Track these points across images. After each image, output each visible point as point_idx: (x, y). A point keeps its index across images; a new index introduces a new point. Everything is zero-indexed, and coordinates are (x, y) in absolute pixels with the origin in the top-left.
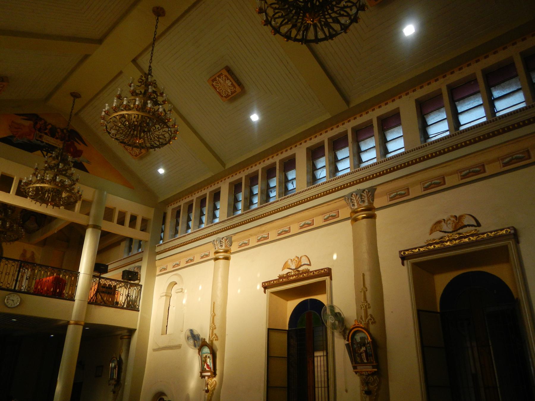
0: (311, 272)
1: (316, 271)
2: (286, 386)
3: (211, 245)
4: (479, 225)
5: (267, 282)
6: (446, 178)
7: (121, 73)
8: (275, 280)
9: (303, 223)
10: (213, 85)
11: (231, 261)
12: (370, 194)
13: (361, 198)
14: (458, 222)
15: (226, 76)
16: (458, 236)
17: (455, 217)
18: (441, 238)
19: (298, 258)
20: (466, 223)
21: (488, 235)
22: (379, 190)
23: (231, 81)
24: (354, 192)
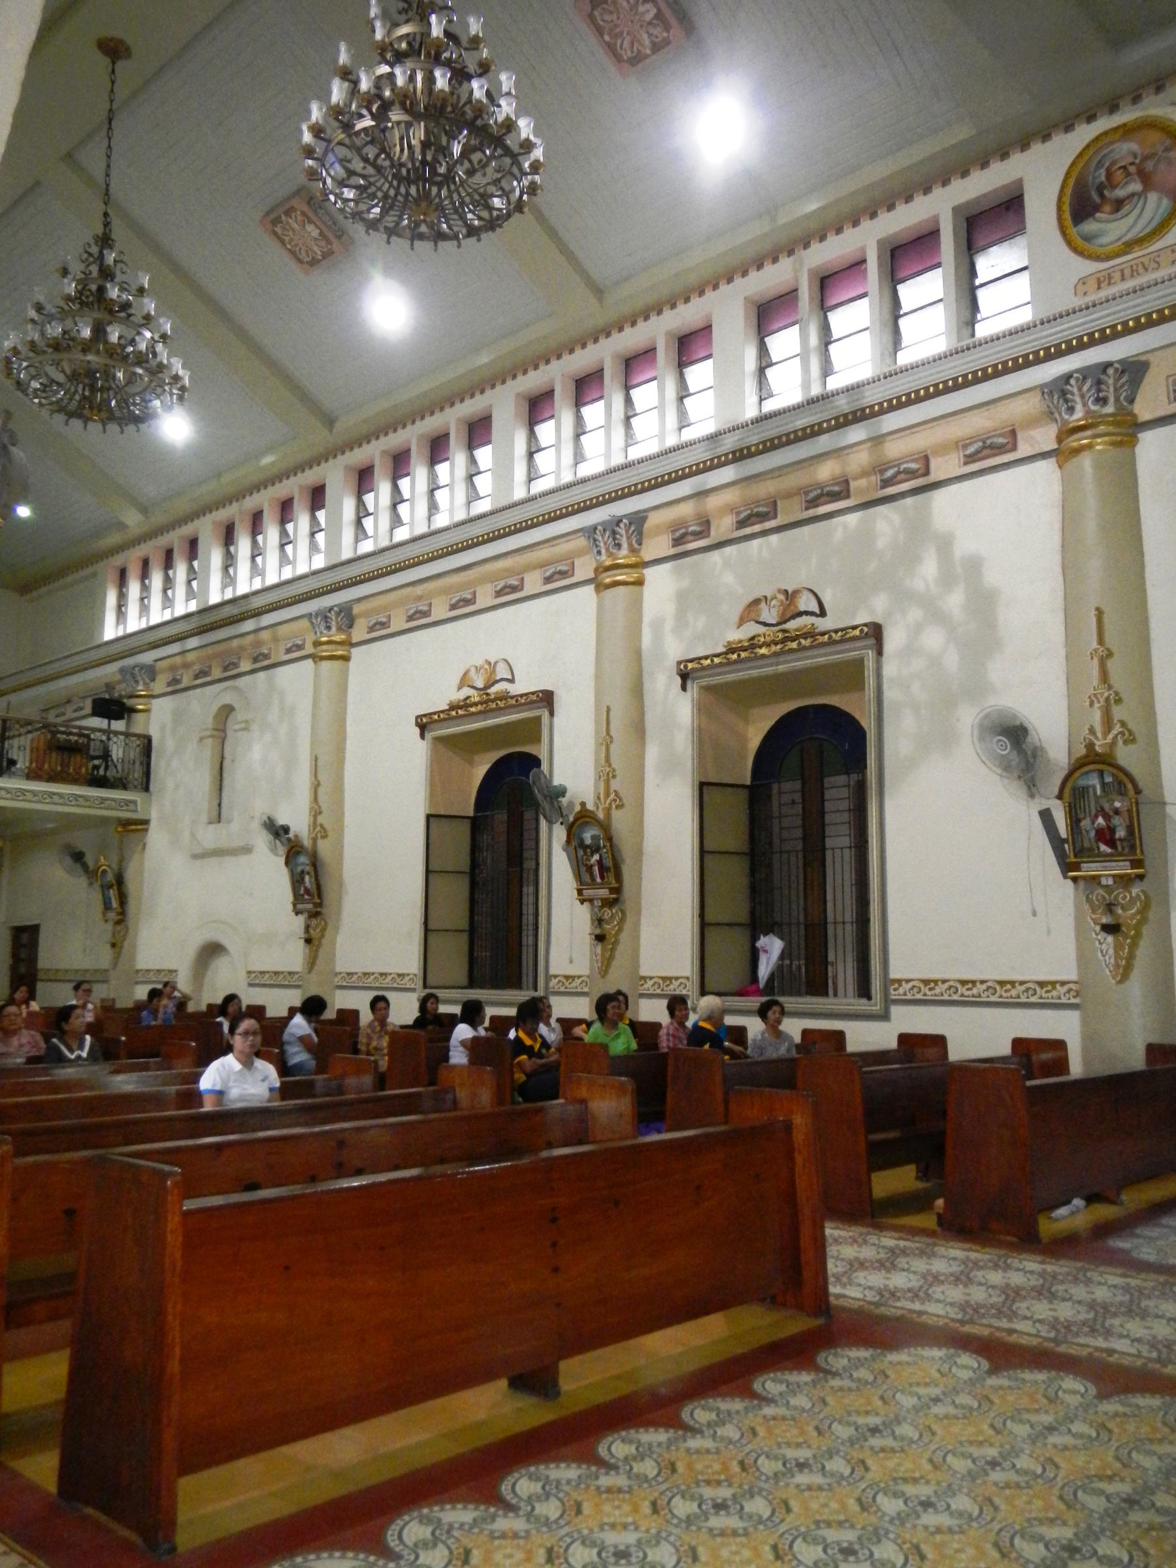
0: (512, 697)
1: (521, 696)
2: (467, 927)
3: (305, 623)
4: (823, 613)
5: (425, 715)
6: (779, 503)
7: (38, 183)
8: (442, 712)
9: (501, 584)
10: (275, 233)
11: (353, 665)
12: (633, 528)
13: (614, 539)
14: (789, 605)
15: (303, 214)
16: (781, 635)
17: (786, 592)
18: (753, 638)
19: (490, 664)
20: (802, 608)
21: (830, 637)
22: (654, 520)
23: (317, 227)
24: (599, 524)
